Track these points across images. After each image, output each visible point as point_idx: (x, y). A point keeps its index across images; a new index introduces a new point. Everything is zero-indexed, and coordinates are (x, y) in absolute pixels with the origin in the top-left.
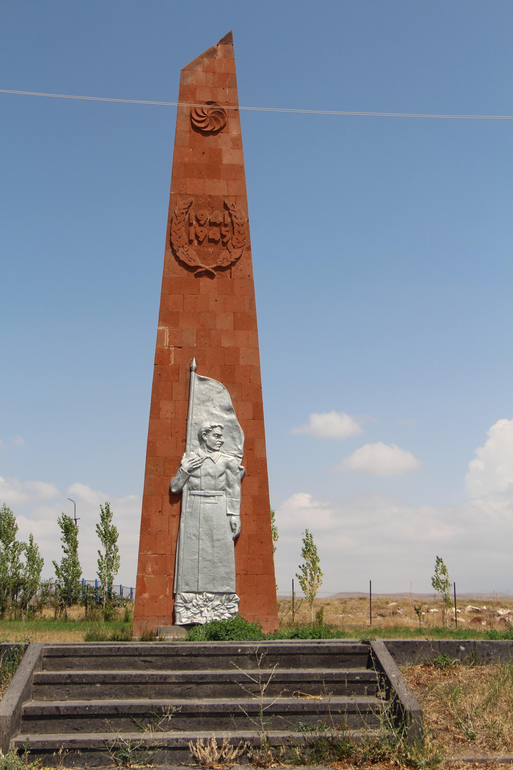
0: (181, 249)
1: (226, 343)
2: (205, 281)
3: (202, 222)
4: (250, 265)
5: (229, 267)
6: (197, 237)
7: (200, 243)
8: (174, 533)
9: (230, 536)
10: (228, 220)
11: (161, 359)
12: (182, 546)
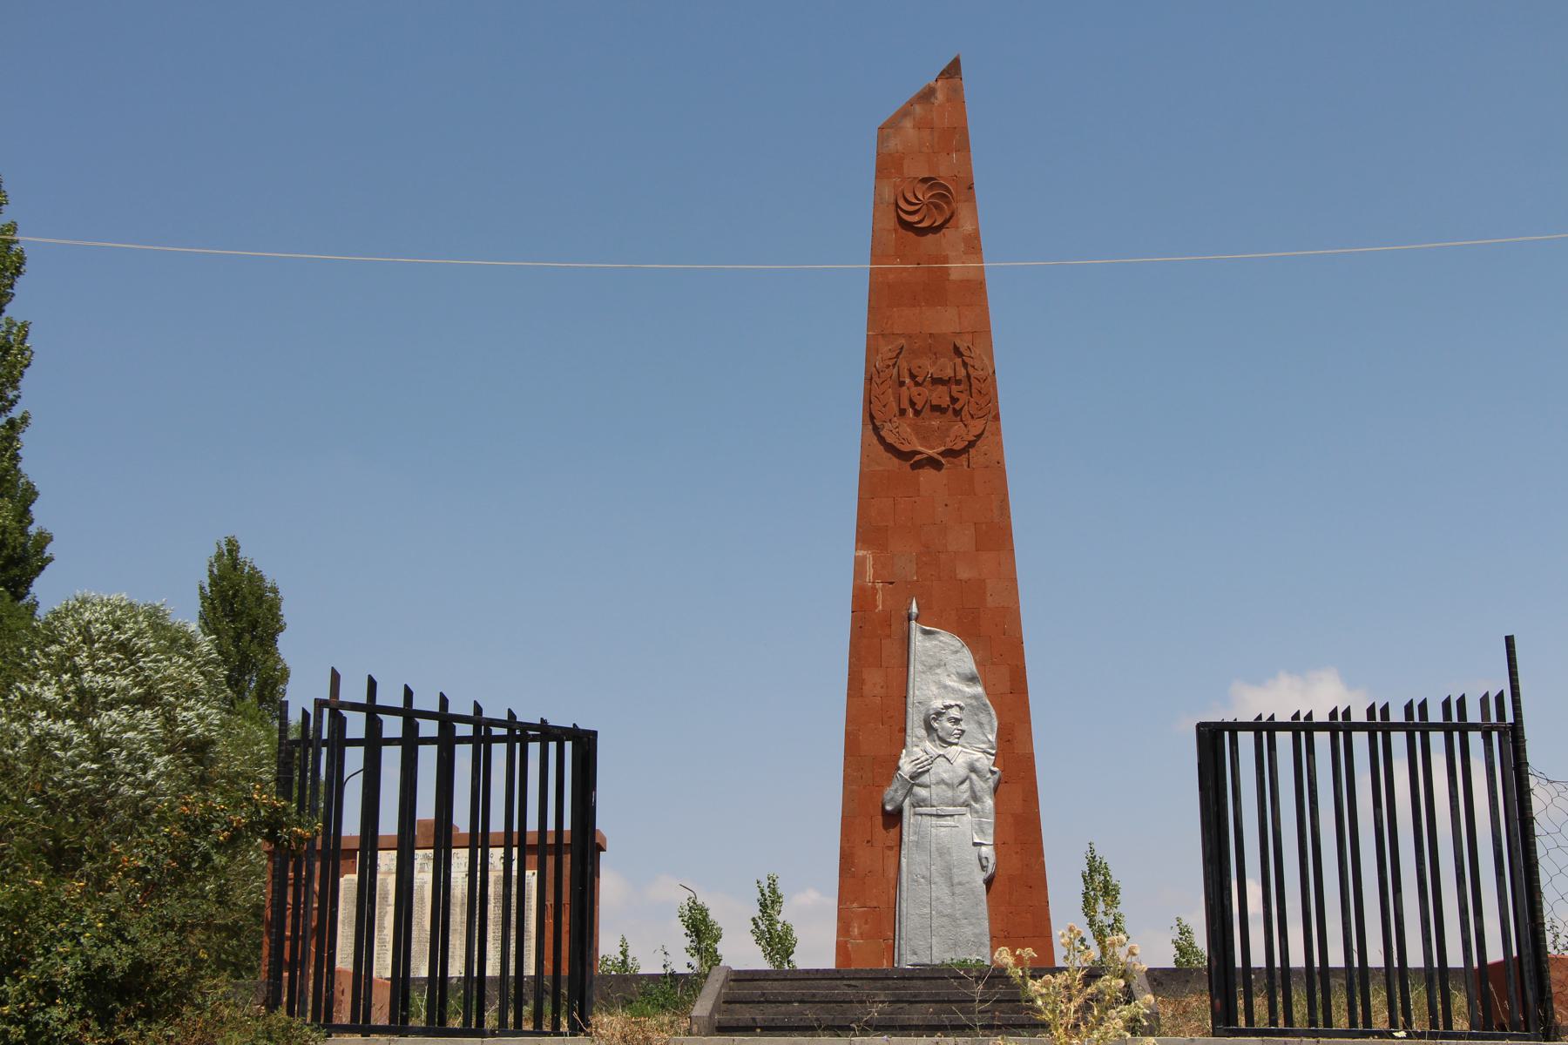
0: (888, 425)
1: (964, 573)
2: (927, 474)
3: (919, 379)
4: (999, 445)
5: (965, 450)
6: (912, 404)
7: (917, 413)
8: (892, 874)
9: (979, 878)
10: (962, 373)
11: (862, 602)
12: (904, 895)
